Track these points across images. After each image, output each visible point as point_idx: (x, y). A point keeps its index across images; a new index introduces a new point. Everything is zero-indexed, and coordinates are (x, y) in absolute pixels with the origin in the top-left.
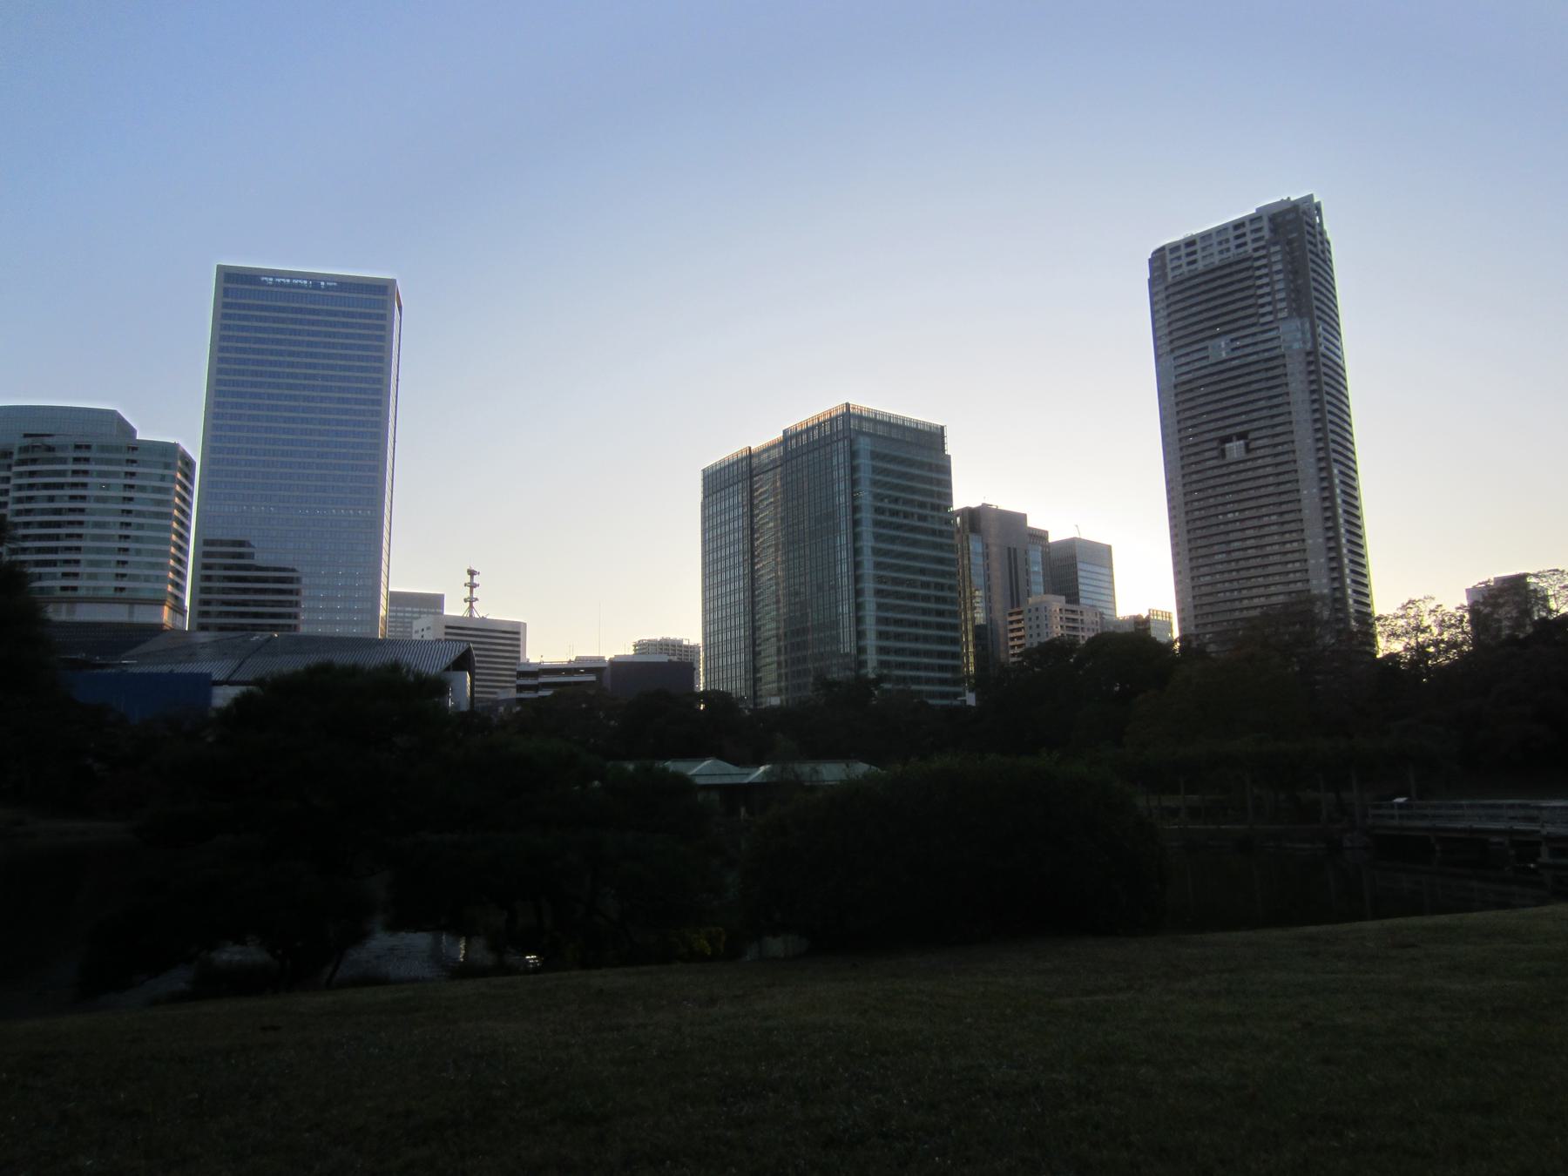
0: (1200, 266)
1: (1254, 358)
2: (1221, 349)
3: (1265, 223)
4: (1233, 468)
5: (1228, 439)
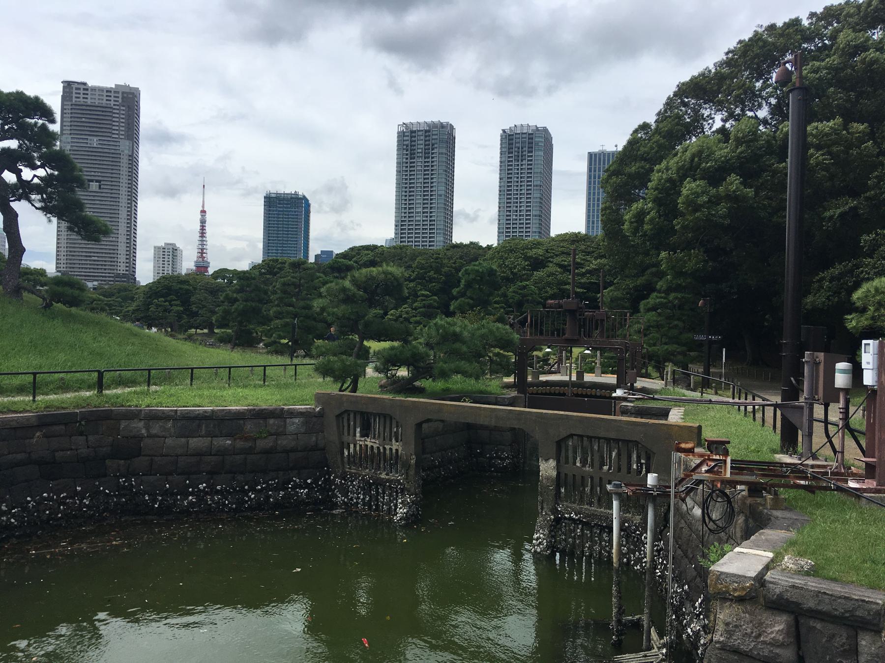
0: (89, 101)
2: (95, 142)
3: (120, 95)
5: (92, 181)
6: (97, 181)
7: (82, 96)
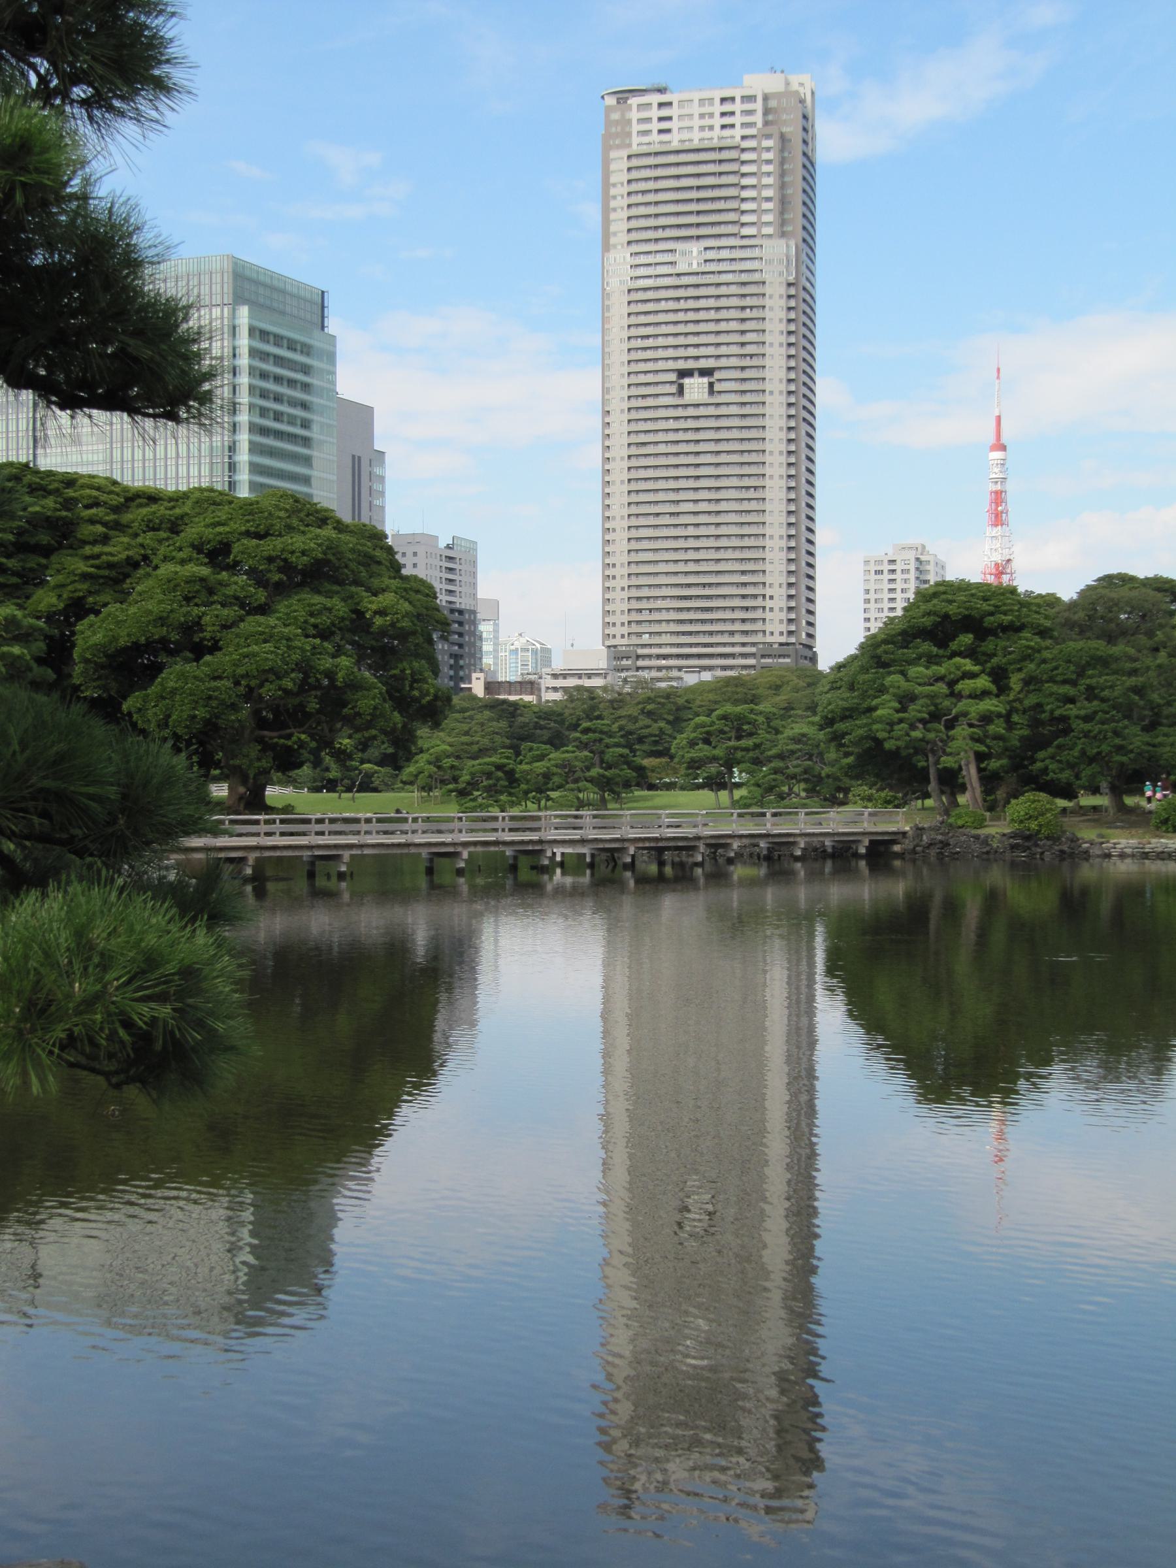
1: (729, 278)
2: (691, 256)
3: (758, 106)
4: (691, 412)
6: (704, 372)
7: (655, 126)
